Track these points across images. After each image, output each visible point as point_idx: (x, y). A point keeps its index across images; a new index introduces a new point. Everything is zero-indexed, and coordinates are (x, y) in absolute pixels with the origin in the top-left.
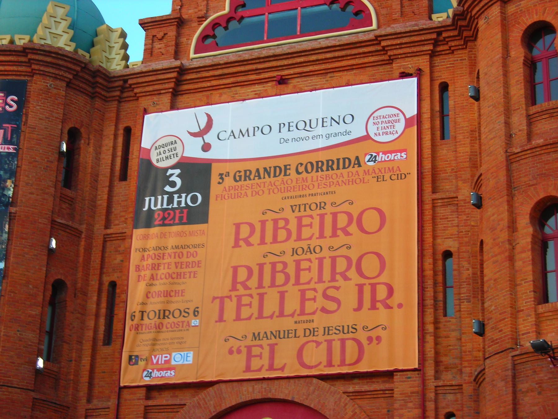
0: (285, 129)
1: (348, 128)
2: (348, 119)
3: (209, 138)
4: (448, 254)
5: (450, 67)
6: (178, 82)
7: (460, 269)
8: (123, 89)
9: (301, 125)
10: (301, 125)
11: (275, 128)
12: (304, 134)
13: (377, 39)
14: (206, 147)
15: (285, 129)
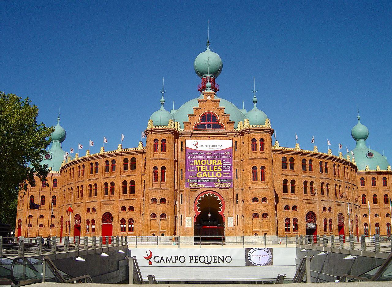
0: (210, 146)
1: (221, 147)
2: (221, 146)
3: (197, 146)
4: (237, 170)
5: (238, 139)
6: (191, 135)
7: (239, 173)
8: (181, 135)
9: (213, 146)
10: (213, 146)
11: (209, 146)
12: (214, 147)
13: (226, 133)
14: (197, 148)
15: (210, 146)
